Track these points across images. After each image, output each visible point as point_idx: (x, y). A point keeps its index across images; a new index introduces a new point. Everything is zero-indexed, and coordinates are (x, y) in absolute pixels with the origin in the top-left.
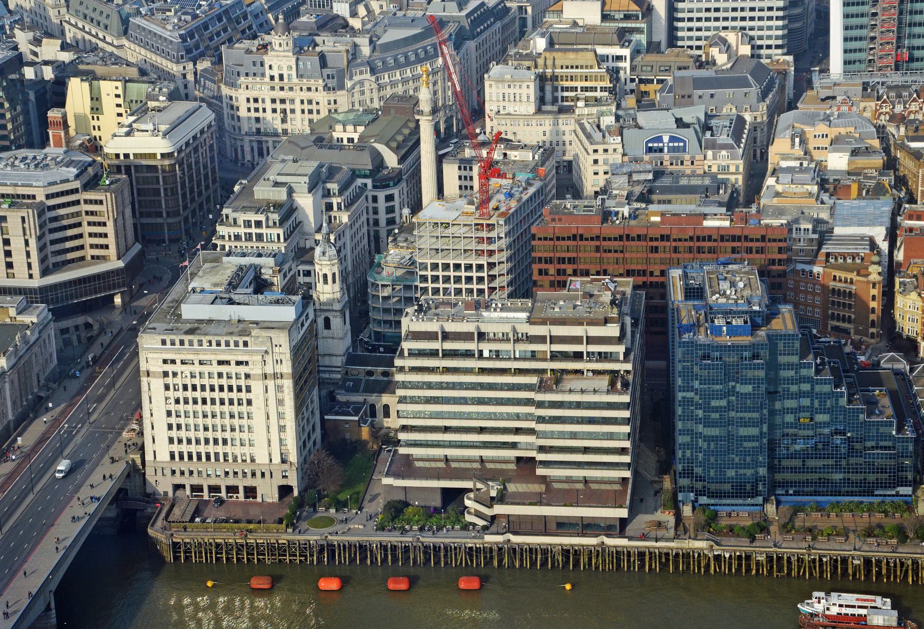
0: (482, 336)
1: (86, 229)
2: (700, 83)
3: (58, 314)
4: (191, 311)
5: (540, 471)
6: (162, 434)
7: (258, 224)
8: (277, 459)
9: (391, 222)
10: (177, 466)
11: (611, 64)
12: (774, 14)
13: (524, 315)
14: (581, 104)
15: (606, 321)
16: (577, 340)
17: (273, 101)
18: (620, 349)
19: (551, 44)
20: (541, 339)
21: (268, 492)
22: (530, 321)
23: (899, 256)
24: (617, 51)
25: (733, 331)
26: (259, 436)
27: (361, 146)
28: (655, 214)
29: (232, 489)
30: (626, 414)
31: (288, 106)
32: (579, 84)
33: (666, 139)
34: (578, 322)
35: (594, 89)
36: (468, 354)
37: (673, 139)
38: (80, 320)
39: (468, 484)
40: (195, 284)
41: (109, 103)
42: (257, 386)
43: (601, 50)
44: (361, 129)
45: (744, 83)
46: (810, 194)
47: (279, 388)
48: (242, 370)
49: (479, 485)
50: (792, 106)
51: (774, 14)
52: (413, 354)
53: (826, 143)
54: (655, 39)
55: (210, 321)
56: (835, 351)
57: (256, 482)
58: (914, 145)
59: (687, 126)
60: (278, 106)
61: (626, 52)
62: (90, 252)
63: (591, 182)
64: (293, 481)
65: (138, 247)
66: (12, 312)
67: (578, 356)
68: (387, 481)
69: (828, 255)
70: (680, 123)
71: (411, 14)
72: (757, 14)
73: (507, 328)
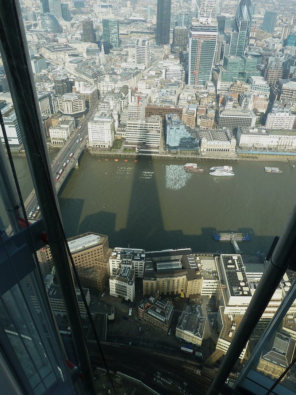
1: (79, 105)
2: (170, 85)
4: (95, 119)
5: (147, 144)
7: (105, 105)
10: (94, 142)
12: (180, 75)
13: (145, 121)
16: (153, 125)
17: (106, 85)
21: (107, 146)
23: (198, 113)
24: (158, 79)
27: (120, 93)
29: (102, 146)
31: (108, 86)
32: (152, 84)
33: (165, 94)
36: (137, 127)
37: (166, 94)
39: (136, 146)
41: (81, 85)
42: (105, 131)
44: (119, 90)
45: (176, 85)
48: (103, 128)
51: (180, 75)
54: (163, 78)
56: (189, 127)
59: (168, 92)
60: (107, 86)
61: (159, 79)
62: (79, 109)
63: (153, 100)
66: (69, 118)
67: (153, 128)
68: (124, 145)
71: (126, 72)
72: (178, 74)
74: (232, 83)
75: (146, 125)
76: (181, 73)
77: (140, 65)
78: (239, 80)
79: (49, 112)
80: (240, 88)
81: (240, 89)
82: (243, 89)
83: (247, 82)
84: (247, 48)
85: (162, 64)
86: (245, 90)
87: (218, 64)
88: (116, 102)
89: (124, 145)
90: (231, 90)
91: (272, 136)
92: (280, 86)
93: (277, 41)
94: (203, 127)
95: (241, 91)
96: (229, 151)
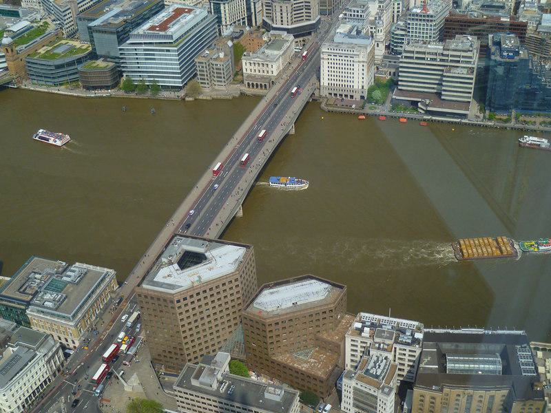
0: (429, 53)
1: (304, 11)
3: (296, 37)
6: (326, 77)
8: (360, 88)
9: (398, 12)
15: (469, 51)
16: (459, 56)
21: (357, 97)
22: (444, 49)
25: (509, 57)
26: (356, 80)
29: (346, 96)
34: (460, 51)
36: (423, 59)
38: (301, 39)
39: (420, 100)
40: (338, 31)
47: (363, 66)
48: (352, 59)
52: (406, 57)
55: (342, 43)
57: (354, 94)
64: (366, 95)
65: (319, 17)
69: (539, 32)
75: (443, 55)
79: (244, 23)
88: (382, 5)
89: (394, 97)
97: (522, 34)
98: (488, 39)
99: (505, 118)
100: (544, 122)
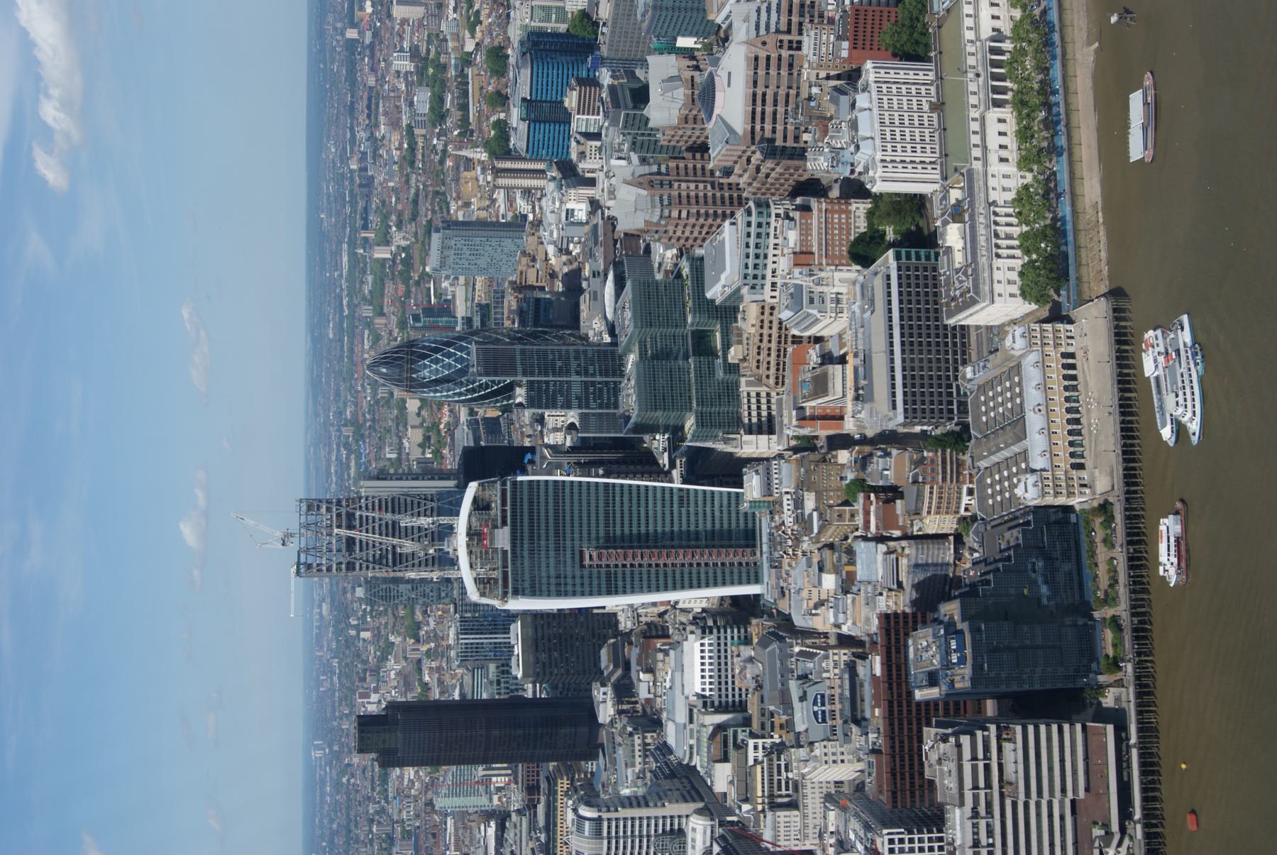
5: (1082, 794)
11: (760, 754)
12: (722, 635)
13: (957, 811)
14: (790, 775)
15: (959, 745)
16: (975, 770)
18: (979, 733)
19: (746, 800)
20: (976, 798)
22: (962, 804)
23: (897, 533)
25: (961, 647)
28: (873, 713)
30: (1031, 728)
32: (776, 778)
33: (816, 708)
35: (779, 766)
43: (751, 762)
46: (854, 600)
49: (1097, 844)
50: (788, 619)
51: (722, 635)
53: (815, 591)
58: (816, 530)
59: (805, 692)
61: (751, 742)
70: (803, 698)
73: (969, 824)
74: (743, 380)
76: (715, 631)
77: (689, 840)
78: (727, 346)
80: (761, 341)
81: (766, 338)
82: (766, 324)
83: (735, 310)
84: (591, 333)
85: (681, 729)
86: (771, 314)
87: (666, 454)
90: (777, 383)
91: (977, 152)
92: (740, 157)
93: (554, 203)
94: (965, 500)
95: (775, 332)
96: (1072, 356)
97: (906, 623)
98: (927, 703)
99: (1109, 635)
100: (1105, 541)
